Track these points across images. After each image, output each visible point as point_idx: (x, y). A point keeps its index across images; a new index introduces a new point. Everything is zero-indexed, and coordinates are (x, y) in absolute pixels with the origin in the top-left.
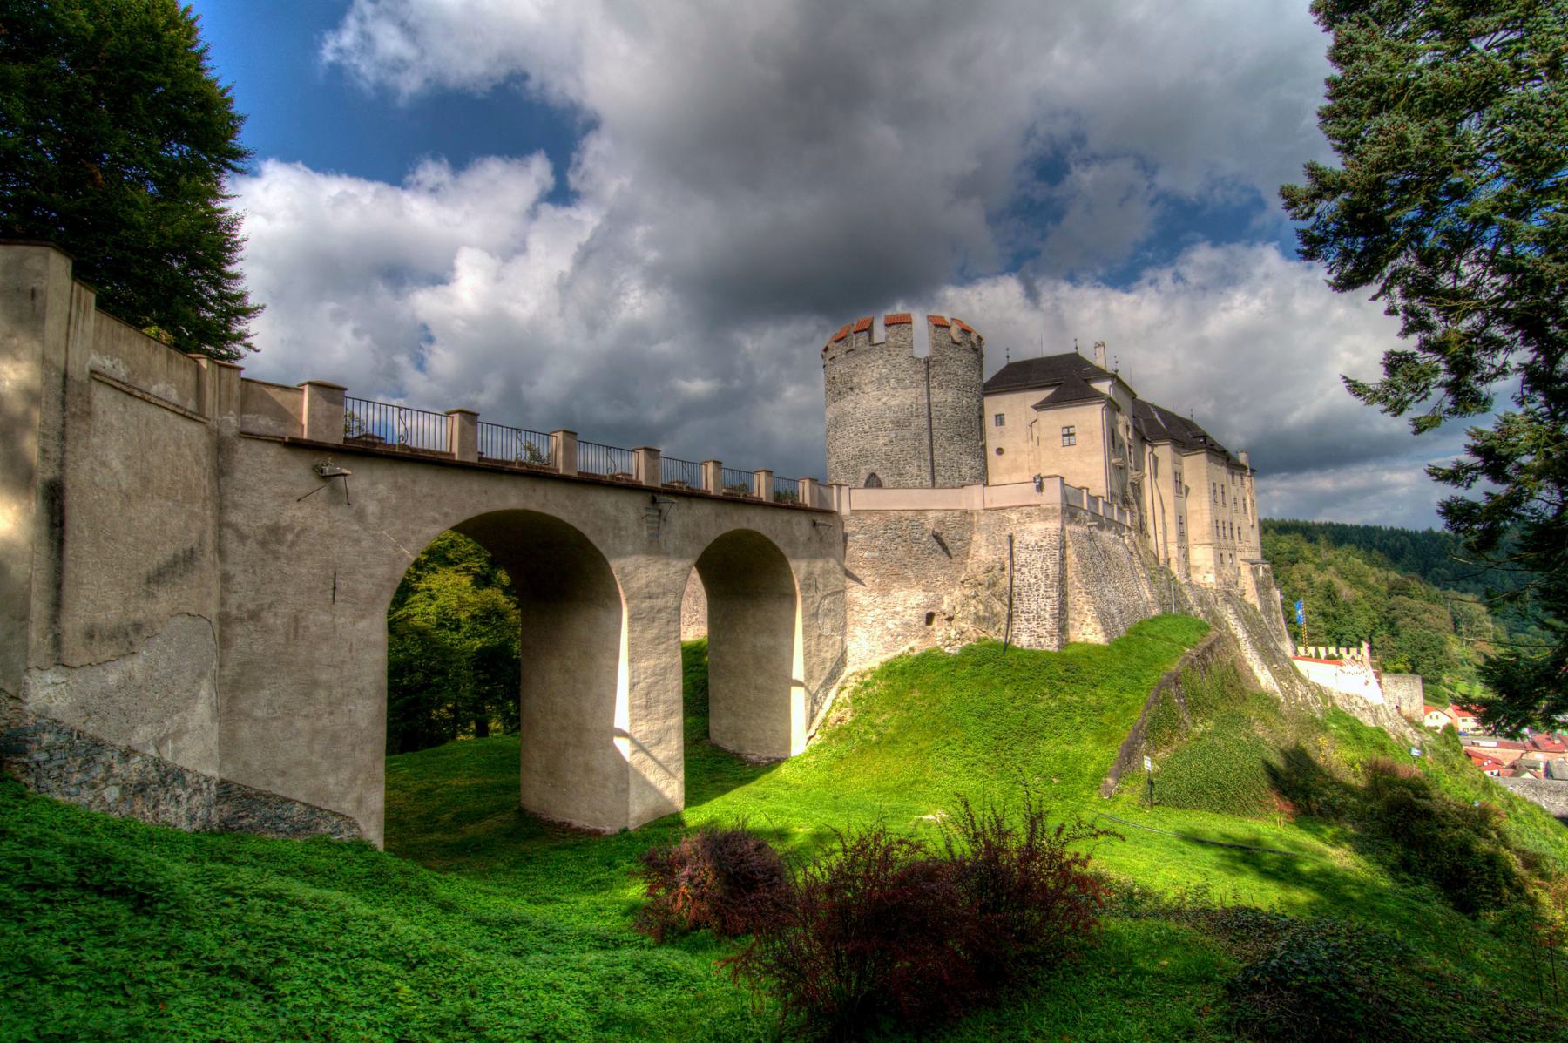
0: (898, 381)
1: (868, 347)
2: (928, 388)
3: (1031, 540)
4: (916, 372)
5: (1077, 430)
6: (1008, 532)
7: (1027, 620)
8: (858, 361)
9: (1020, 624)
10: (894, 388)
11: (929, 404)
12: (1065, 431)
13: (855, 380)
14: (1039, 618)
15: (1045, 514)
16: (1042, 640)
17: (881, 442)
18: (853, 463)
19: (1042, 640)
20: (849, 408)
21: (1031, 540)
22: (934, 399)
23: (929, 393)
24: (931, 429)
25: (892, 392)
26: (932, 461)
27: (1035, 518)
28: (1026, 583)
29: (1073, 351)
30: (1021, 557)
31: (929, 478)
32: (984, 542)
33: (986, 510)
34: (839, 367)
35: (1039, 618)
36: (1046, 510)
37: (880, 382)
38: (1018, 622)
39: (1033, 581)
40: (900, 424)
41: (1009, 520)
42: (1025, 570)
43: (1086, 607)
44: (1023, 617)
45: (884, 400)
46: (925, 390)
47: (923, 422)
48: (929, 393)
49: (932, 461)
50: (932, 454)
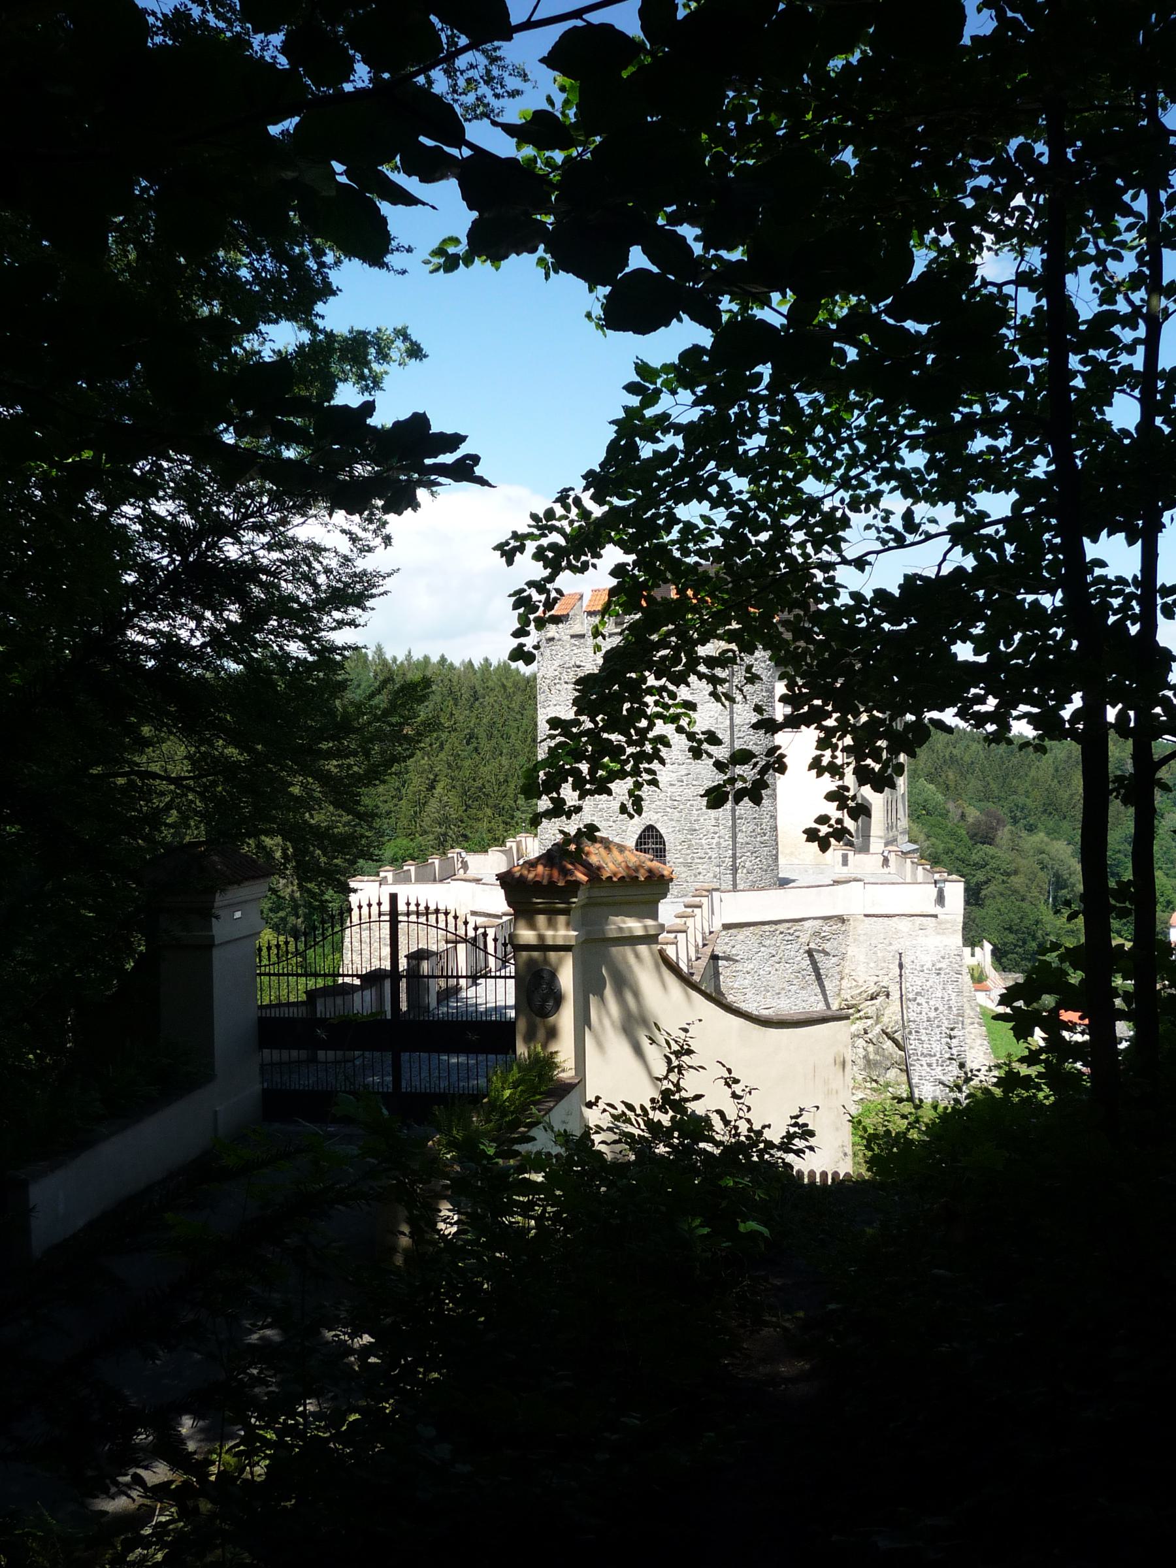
3: (927, 960)
6: (896, 946)
7: (929, 1065)
11: (732, 726)
15: (941, 930)
30: (913, 982)
31: (728, 835)
32: (862, 958)
33: (866, 916)
36: (947, 922)
38: (917, 1067)
39: (933, 1014)
41: (897, 931)
42: (920, 999)
43: (979, 1042)
44: (924, 1061)
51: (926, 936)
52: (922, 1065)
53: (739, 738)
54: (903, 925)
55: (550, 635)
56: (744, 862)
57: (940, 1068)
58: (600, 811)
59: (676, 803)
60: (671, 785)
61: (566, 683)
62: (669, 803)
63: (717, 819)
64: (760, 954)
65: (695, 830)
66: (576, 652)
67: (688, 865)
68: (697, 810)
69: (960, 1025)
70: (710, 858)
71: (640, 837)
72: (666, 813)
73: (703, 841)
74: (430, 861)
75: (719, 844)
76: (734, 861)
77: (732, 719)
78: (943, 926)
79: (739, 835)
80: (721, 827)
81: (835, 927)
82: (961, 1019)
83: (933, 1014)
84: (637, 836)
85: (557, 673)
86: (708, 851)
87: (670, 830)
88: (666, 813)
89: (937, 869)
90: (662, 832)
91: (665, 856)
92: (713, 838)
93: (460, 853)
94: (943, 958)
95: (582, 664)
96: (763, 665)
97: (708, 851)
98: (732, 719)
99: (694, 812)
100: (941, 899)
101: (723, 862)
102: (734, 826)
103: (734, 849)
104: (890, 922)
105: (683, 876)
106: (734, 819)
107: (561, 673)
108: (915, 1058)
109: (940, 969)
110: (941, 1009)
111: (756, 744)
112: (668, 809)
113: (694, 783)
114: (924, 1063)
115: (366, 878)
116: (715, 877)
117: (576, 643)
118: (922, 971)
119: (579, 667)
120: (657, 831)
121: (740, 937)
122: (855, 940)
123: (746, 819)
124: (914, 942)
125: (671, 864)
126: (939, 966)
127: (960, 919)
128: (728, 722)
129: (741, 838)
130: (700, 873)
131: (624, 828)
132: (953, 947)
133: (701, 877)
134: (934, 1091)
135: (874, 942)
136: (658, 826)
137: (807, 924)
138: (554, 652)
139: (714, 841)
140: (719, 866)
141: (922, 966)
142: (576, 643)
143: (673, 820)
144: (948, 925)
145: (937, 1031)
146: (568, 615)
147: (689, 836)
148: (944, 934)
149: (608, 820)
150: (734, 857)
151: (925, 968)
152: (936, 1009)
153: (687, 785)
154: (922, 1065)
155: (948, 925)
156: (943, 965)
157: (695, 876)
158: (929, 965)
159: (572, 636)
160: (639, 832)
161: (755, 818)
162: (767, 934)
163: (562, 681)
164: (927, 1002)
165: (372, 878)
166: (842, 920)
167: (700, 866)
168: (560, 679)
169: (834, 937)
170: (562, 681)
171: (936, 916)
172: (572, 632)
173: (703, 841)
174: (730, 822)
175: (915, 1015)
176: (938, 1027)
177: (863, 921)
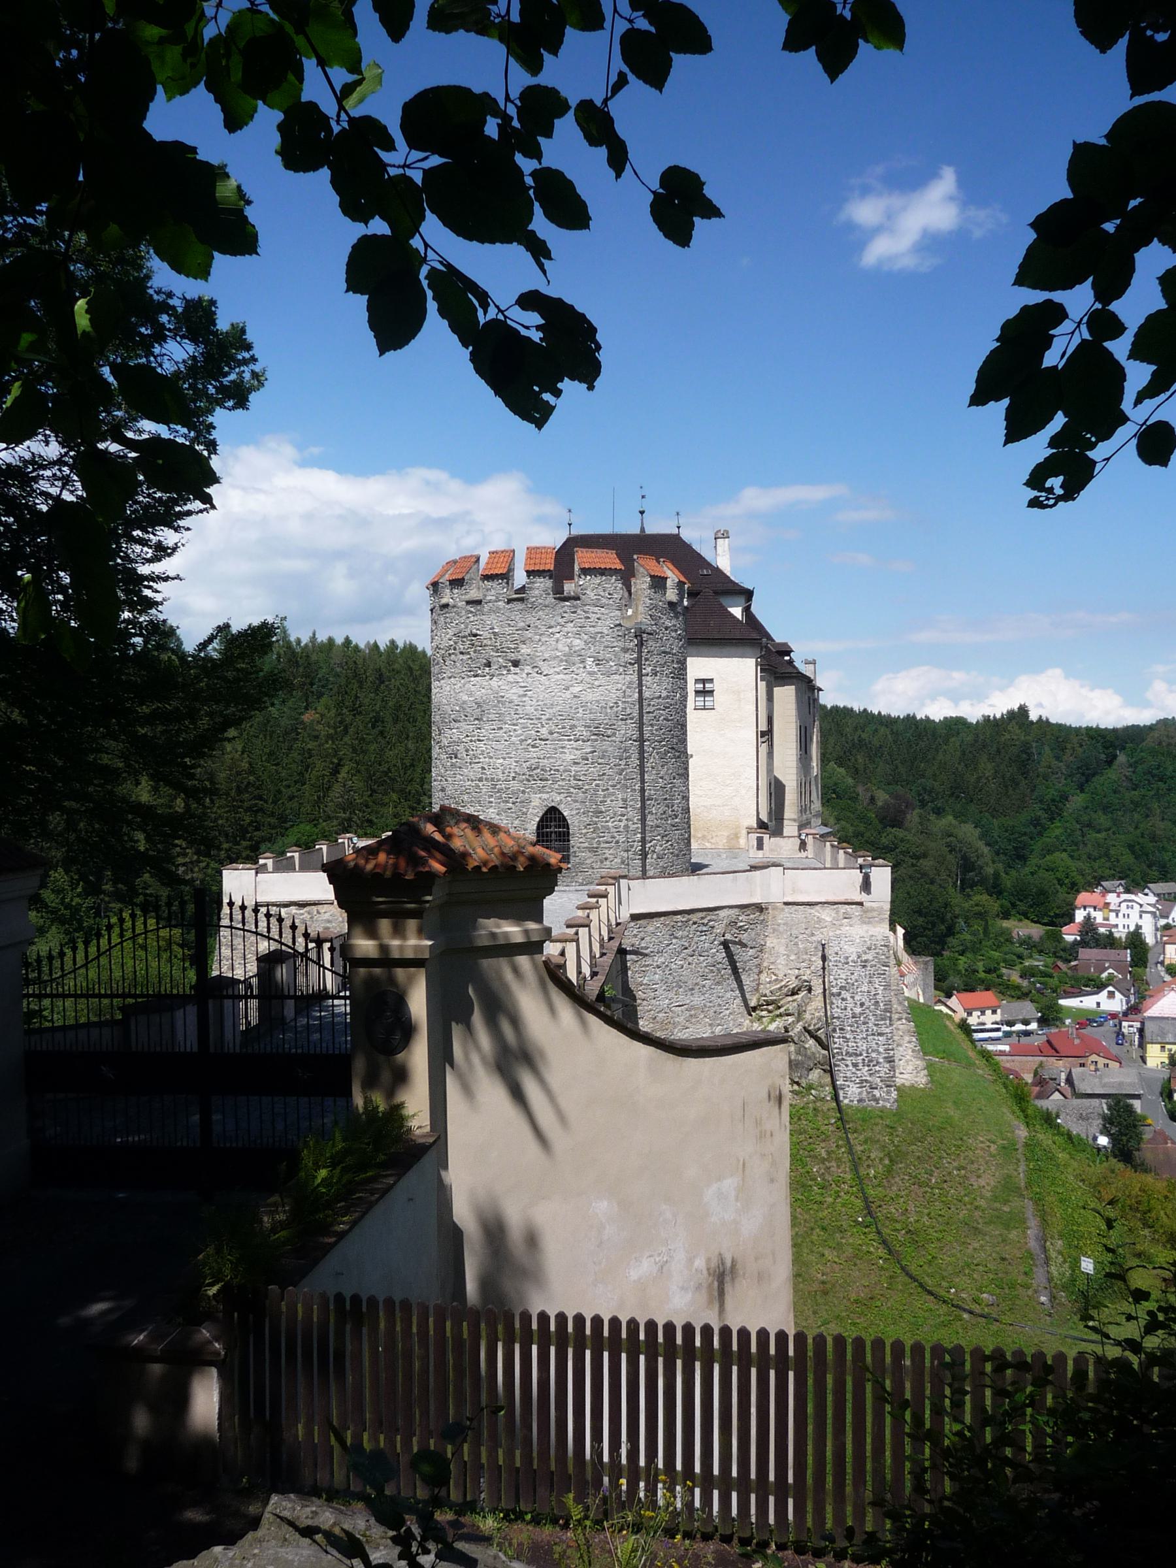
0: (598, 662)
1: (550, 599)
2: (640, 675)
3: (852, 951)
4: (625, 650)
5: (716, 686)
6: (818, 937)
7: (855, 1065)
8: (531, 619)
9: (844, 1070)
10: (590, 673)
11: (641, 699)
12: (700, 686)
13: (525, 650)
14: (870, 1062)
15: (868, 917)
16: (877, 1093)
17: (569, 757)
18: (515, 786)
19: (877, 1093)
20: (513, 693)
21: (852, 951)
22: (646, 694)
23: (640, 685)
24: (641, 740)
25: (588, 679)
26: (643, 790)
27: (855, 920)
28: (849, 1013)
29: (675, 531)
30: (838, 976)
32: (782, 950)
33: (786, 904)
34: (491, 620)
35: (870, 1062)
36: (873, 910)
37: (570, 659)
38: (842, 1067)
39: (858, 1010)
40: (598, 732)
41: (820, 920)
42: (844, 994)
43: (907, 1038)
44: (849, 1060)
45: (576, 689)
46: (635, 677)
47: (628, 730)
48: (640, 685)
49: (643, 790)
50: (643, 781)
51: (851, 926)
52: (847, 1066)
53: (649, 712)
54: (827, 915)
55: (444, 601)
56: (655, 845)
57: (867, 1068)
58: (498, 792)
59: (580, 783)
60: (575, 763)
61: (462, 653)
62: (573, 782)
63: (625, 800)
64: (671, 947)
65: (602, 812)
66: (472, 619)
67: (593, 850)
68: (603, 791)
69: (888, 1022)
70: (617, 842)
71: (542, 820)
72: (570, 794)
73: (610, 824)
74: (317, 847)
75: (626, 826)
76: (644, 846)
77: (640, 692)
78: (870, 915)
79: (649, 817)
80: (629, 809)
81: (752, 916)
82: (888, 1014)
83: (858, 1010)
84: (538, 819)
85: (451, 643)
86: (616, 834)
87: (574, 812)
88: (570, 794)
89: (861, 853)
90: (565, 814)
91: (569, 841)
92: (620, 821)
93: (350, 839)
94: (869, 949)
95: (478, 632)
96: (673, 634)
97: (616, 834)
98: (640, 692)
99: (600, 793)
100: (866, 886)
101: (632, 846)
102: (643, 807)
103: (643, 832)
104: (813, 911)
105: (588, 861)
106: (643, 801)
107: (456, 643)
108: (840, 1057)
109: (866, 961)
110: (867, 1004)
111: (668, 720)
112: (572, 790)
113: (600, 761)
114: (849, 1063)
115: (241, 866)
116: (623, 862)
117: (472, 609)
118: (847, 963)
119: (475, 635)
120: (560, 813)
121: (650, 929)
122: (774, 930)
123: (656, 800)
124: (838, 932)
125: (575, 849)
126: (864, 957)
127: (887, 906)
128: (637, 695)
129: (651, 821)
130: (606, 859)
131: (524, 810)
132: (880, 938)
133: (608, 863)
134: (860, 1093)
135: (794, 932)
136: (561, 808)
137: (722, 914)
138: (448, 620)
139: (622, 824)
140: (627, 851)
141: (847, 958)
142: (472, 609)
143: (577, 801)
144: (875, 914)
145: (864, 1028)
146: (463, 579)
147: (594, 819)
148: (869, 923)
149: (507, 802)
150: (643, 841)
151: (850, 959)
152: (862, 1005)
153: (592, 763)
154: (847, 1066)
155: (875, 914)
156: (869, 957)
157: (602, 862)
158: (854, 957)
159: (468, 603)
160: (540, 814)
161: (666, 799)
162: (679, 924)
163: (457, 652)
164: (853, 997)
165: (248, 866)
166: (760, 908)
167: (606, 851)
168: (455, 649)
169: (752, 926)
170: (457, 652)
171: (861, 904)
172: (467, 597)
173: (610, 824)
174: (639, 803)
175: (839, 1010)
176: (864, 1023)
177: (783, 909)
